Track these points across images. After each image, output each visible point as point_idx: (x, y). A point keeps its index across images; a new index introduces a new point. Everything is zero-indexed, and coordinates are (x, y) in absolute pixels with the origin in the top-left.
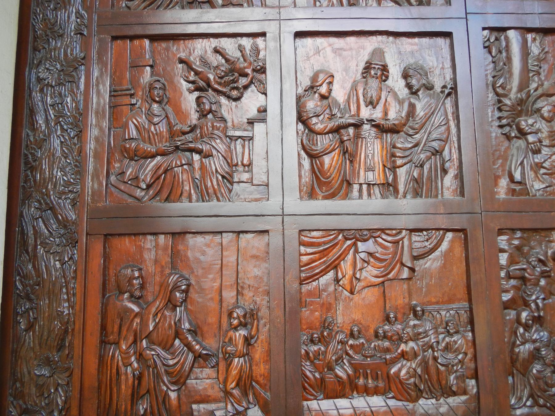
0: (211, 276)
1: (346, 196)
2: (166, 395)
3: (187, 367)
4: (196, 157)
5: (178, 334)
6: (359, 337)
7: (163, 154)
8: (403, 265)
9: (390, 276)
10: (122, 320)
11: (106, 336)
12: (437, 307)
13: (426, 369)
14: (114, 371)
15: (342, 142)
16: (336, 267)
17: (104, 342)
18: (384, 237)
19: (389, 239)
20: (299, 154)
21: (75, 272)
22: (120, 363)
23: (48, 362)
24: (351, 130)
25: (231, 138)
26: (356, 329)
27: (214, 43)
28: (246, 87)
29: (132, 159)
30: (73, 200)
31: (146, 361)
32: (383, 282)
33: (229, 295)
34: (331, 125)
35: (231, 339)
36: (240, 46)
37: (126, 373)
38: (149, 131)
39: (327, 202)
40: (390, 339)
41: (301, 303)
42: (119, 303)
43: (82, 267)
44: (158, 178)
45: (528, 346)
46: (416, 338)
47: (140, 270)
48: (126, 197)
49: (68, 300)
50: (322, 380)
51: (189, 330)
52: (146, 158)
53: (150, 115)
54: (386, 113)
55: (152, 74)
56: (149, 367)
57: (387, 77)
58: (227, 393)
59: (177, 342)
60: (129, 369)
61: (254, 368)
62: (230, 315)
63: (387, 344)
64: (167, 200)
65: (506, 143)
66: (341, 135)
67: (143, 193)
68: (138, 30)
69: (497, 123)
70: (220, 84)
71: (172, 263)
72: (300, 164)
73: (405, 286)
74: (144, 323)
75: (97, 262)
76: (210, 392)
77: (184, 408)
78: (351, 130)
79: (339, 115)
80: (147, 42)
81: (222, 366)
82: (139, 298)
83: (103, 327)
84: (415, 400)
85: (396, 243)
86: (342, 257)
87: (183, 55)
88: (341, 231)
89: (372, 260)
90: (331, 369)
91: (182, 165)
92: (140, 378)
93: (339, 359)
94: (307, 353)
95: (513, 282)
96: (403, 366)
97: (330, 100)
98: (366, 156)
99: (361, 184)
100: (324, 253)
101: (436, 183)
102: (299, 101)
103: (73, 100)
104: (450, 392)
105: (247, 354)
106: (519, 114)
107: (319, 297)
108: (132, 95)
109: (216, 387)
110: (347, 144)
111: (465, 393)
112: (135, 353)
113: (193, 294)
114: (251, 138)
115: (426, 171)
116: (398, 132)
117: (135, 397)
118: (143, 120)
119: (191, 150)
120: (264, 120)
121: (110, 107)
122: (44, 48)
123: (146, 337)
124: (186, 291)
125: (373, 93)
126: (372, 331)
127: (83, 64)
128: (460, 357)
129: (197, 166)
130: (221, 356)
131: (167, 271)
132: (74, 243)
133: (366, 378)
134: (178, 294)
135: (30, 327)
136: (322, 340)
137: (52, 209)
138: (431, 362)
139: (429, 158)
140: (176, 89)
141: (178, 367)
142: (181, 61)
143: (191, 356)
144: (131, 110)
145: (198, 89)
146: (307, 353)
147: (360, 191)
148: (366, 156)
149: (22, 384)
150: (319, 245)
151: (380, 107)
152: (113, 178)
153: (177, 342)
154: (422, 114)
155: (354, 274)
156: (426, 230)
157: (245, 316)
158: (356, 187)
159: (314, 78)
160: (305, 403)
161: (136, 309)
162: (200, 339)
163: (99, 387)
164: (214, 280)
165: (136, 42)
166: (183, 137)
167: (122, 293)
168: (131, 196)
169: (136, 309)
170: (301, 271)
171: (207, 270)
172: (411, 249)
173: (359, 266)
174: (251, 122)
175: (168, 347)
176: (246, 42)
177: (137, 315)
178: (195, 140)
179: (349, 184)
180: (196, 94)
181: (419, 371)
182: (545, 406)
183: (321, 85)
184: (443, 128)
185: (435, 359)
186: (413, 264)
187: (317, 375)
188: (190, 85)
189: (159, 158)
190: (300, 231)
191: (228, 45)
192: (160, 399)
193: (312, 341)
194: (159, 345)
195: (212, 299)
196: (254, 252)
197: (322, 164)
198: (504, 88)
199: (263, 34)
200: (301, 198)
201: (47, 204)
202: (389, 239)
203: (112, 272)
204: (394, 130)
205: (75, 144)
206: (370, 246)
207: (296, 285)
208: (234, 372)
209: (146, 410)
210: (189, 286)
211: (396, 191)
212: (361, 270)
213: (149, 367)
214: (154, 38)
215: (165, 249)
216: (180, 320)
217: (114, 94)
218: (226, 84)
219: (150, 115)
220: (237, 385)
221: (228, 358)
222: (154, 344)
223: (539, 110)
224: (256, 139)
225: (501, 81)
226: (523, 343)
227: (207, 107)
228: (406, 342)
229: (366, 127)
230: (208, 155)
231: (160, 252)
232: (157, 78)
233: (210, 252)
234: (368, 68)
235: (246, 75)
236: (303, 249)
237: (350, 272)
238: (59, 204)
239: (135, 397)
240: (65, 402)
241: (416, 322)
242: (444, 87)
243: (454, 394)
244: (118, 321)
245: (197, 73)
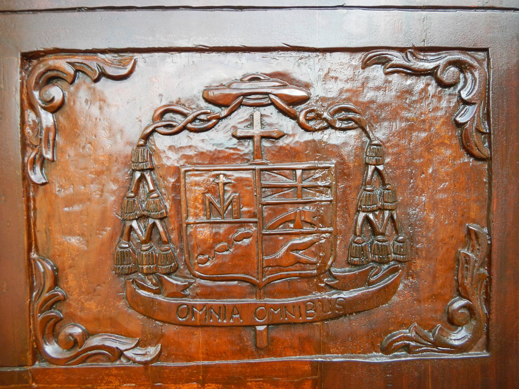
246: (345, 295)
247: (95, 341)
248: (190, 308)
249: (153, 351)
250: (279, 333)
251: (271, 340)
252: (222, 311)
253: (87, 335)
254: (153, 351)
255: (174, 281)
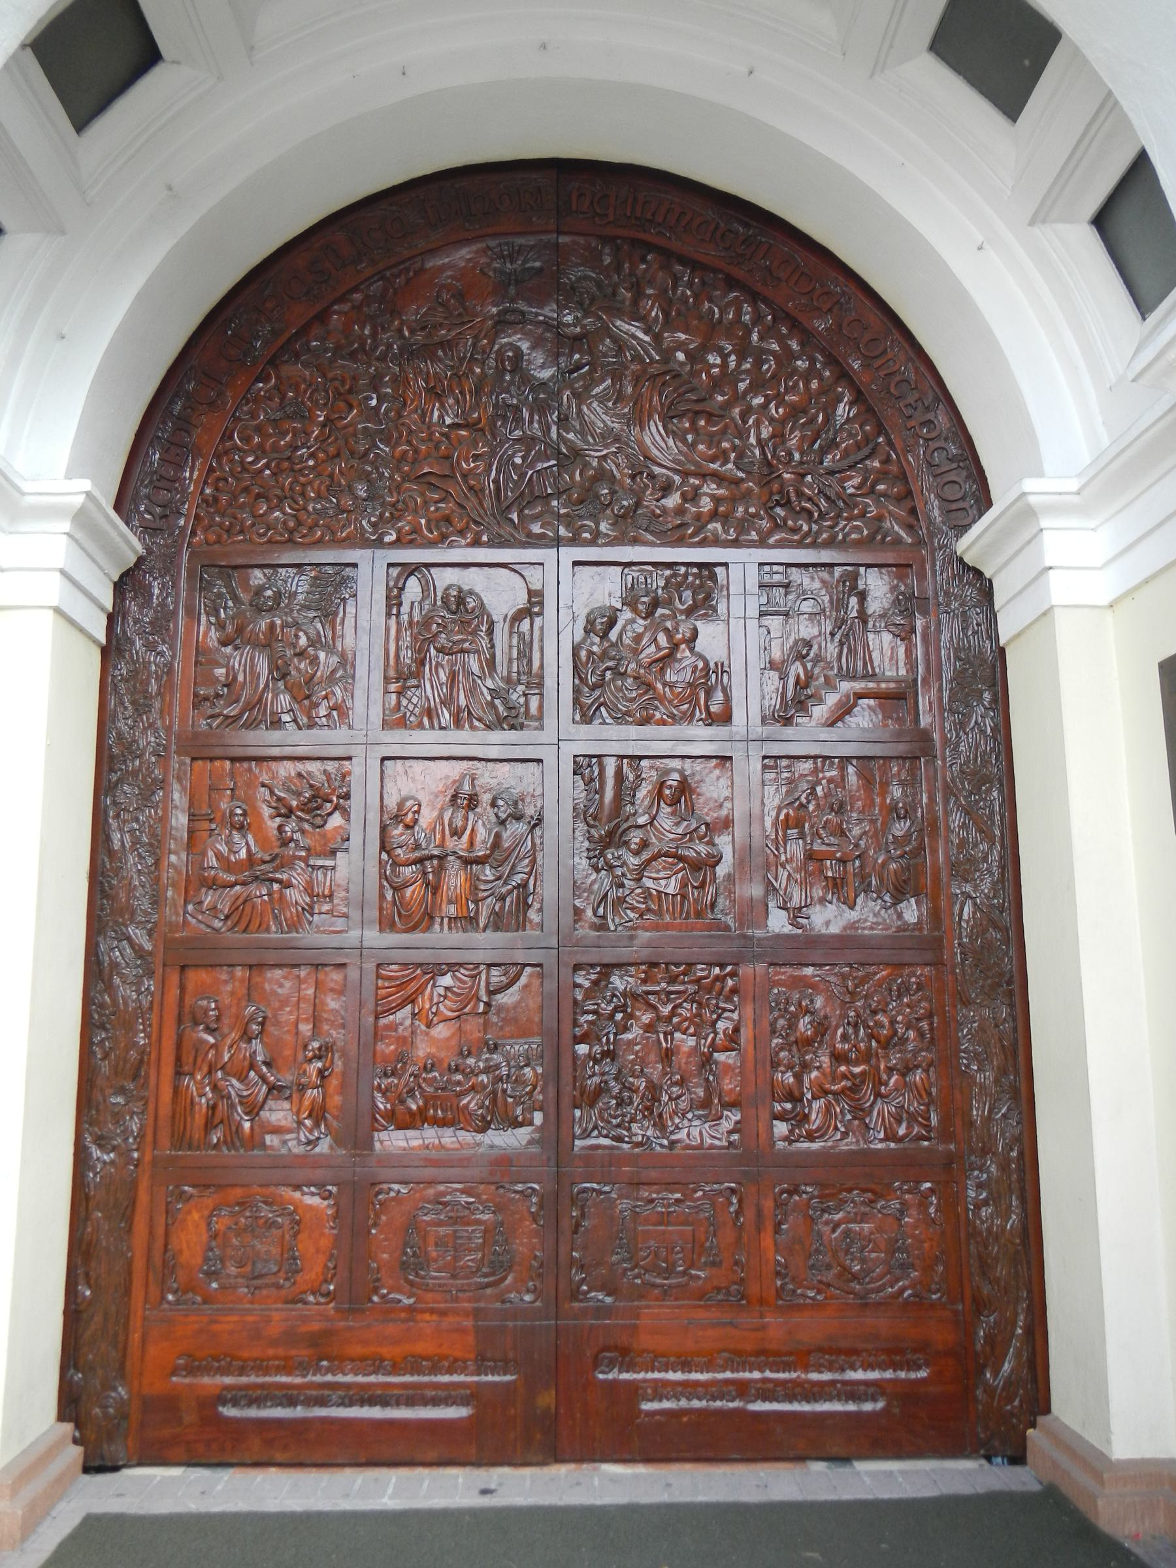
0: (288, 1009)
1: (428, 929)
2: (239, 1126)
3: (261, 1098)
4: (276, 886)
5: (252, 1066)
6: (431, 1071)
7: (244, 884)
8: (479, 1000)
9: (467, 1010)
10: (197, 1051)
11: (181, 1066)
12: (511, 1041)
13: (494, 1101)
14: (189, 1100)
15: (425, 873)
16: (413, 1002)
17: (179, 1073)
18: (462, 971)
19: (467, 973)
20: (381, 887)
21: (151, 1002)
22: (195, 1094)
23: (122, 1091)
24: (435, 862)
25: (313, 867)
26: (430, 1061)
27: (300, 766)
28: (330, 814)
29: (210, 888)
30: (150, 930)
31: (221, 1091)
32: (458, 1017)
33: (306, 1028)
34: (417, 854)
35: (305, 1072)
36: (325, 771)
37: (200, 1104)
38: (228, 859)
39: (405, 936)
40: (463, 1072)
41: (377, 1036)
42: (194, 1035)
43: (158, 998)
44: (237, 908)
45: (597, 1079)
46: (487, 1070)
47: (216, 1001)
48: (202, 927)
49: (144, 1031)
50: (393, 1111)
51: (265, 1063)
52: (225, 887)
53: (229, 842)
54: (471, 843)
55: (232, 797)
56: (223, 1097)
57: (476, 806)
58: (300, 1123)
59: (252, 1073)
60: (203, 1100)
61: (327, 1100)
62: (305, 1047)
63: (459, 1077)
64: (245, 931)
65: (594, 876)
66: (424, 867)
67: (221, 924)
68: (218, 751)
69: (585, 854)
70: (302, 810)
71: (249, 995)
72: (382, 897)
73: (481, 1021)
74: (219, 1055)
75: (174, 993)
76: (283, 1123)
77: (257, 1138)
78: (435, 862)
79: (424, 845)
80: (228, 762)
81: (295, 1097)
82: (215, 1030)
83: (178, 1059)
84: (482, 1130)
85: (473, 977)
86: (420, 990)
87: (265, 778)
88: (420, 965)
89: (449, 994)
90: (402, 1102)
91: (262, 896)
92: (213, 1108)
93: (411, 1092)
94: (379, 1085)
95: (590, 1017)
96: (472, 1099)
97: (417, 828)
98: (448, 888)
99: (442, 918)
100: (401, 986)
101: (518, 917)
102: (383, 829)
103: (150, 826)
104: (516, 1124)
105: (322, 1086)
106: (608, 846)
107: (396, 1030)
108: (211, 821)
109: (289, 1118)
110: (430, 876)
111: (531, 1123)
112: (209, 1084)
113: (270, 1029)
114: (334, 868)
115: (507, 904)
116: (483, 863)
117: (209, 1126)
118: (223, 848)
119: (272, 880)
120: (346, 850)
121: (188, 832)
122: (121, 770)
123: (221, 1068)
124: (262, 1024)
125: (459, 822)
126: (445, 1065)
127: (161, 788)
128: (527, 1089)
129: (276, 896)
130: (295, 1088)
131: (243, 1003)
132: (150, 974)
133: (436, 1111)
134: (254, 1027)
135: (106, 1056)
136: (393, 1074)
137: (129, 939)
138: (499, 1095)
139: (510, 892)
140: (259, 815)
141: (253, 1097)
142: (264, 785)
143: (264, 1087)
144: (210, 836)
145: (279, 815)
146: (379, 1085)
147: (442, 924)
148: (448, 888)
149: (98, 1111)
150: (397, 978)
151: (466, 837)
152: (190, 907)
153: (252, 1073)
154: (506, 845)
155: (431, 1008)
156: (504, 964)
157: (320, 1049)
158: (438, 920)
159: (400, 805)
160: (376, 1134)
161: (211, 1040)
162: (275, 1072)
163: (173, 1117)
164: (290, 1013)
165: (217, 763)
166: (263, 867)
167: (196, 1023)
168: (208, 926)
169: (211, 1040)
170: (377, 1005)
171: (284, 1002)
172: (488, 983)
173: (435, 1000)
174: (333, 853)
175: (243, 1078)
176: (331, 766)
177: (212, 1046)
178: (276, 870)
179: (432, 918)
180: (278, 820)
181: (487, 1103)
182: (606, 1136)
183: (406, 814)
184: (527, 861)
185: (504, 1091)
186: (490, 998)
187: (389, 1106)
188: (272, 811)
189: (238, 887)
190: (379, 965)
191: (314, 767)
192: (234, 1128)
193: (386, 1075)
194: (234, 1076)
195: (288, 1031)
196: (332, 985)
197: (403, 897)
198: (595, 819)
199: (349, 758)
200: (381, 931)
201: (124, 934)
202: (467, 973)
203: (188, 1001)
204: (480, 861)
205: (152, 873)
206: (447, 980)
207: (371, 1019)
208: (306, 1103)
209: (219, 1140)
210: (265, 1018)
211: (478, 924)
212: (438, 1003)
213: (223, 1097)
214: (233, 760)
215: (242, 980)
216: (255, 1052)
217: (193, 818)
218: (308, 812)
219: (229, 842)
220: (309, 1116)
221: (302, 1088)
222: (228, 1074)
223: (627, 843)
224: (338, 869)
225: (591, 810)
226: (590, 1077)
227: (289, 834)
228: (477, 1075)
229: (451, 858)
230: (289, 885)
231: (237, 984)
232: (239, 804)
233: (288, 984)
234: (455, 797)
235: (331, 801)
236: (380, 982)
237: (427, 1006)
238: (135, 934)
239: (209, 1126)
240: (140, 1129)
241: (487, 1056)
242: (532, 817)
243: (521, 1125)
244: (193, 1053)
245: (279, 799)
246: (486, 1280)
247: (392, 1296)
248: (427, 1284)
249: (412, 1301)
250: (460, 1294)
251: (457, 1297)
252: (440, 1285)
253: (389, 1293)
254: (412, 1301)
255: (422, 1273)
